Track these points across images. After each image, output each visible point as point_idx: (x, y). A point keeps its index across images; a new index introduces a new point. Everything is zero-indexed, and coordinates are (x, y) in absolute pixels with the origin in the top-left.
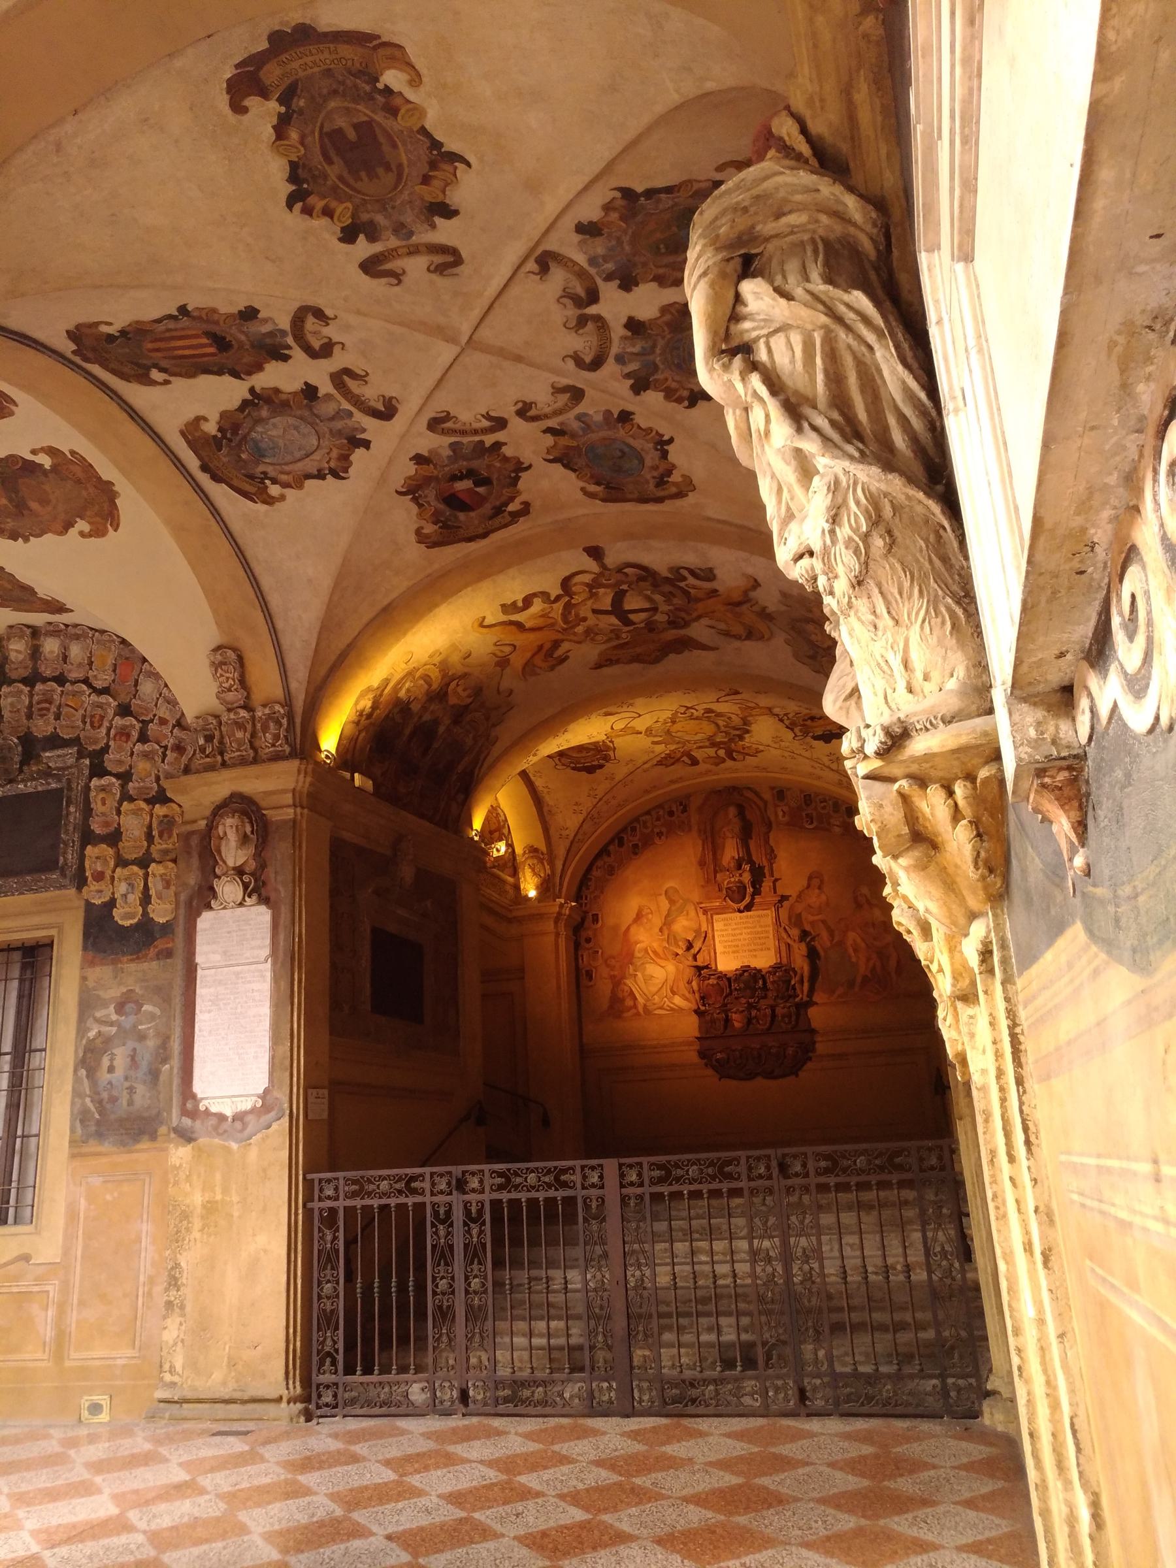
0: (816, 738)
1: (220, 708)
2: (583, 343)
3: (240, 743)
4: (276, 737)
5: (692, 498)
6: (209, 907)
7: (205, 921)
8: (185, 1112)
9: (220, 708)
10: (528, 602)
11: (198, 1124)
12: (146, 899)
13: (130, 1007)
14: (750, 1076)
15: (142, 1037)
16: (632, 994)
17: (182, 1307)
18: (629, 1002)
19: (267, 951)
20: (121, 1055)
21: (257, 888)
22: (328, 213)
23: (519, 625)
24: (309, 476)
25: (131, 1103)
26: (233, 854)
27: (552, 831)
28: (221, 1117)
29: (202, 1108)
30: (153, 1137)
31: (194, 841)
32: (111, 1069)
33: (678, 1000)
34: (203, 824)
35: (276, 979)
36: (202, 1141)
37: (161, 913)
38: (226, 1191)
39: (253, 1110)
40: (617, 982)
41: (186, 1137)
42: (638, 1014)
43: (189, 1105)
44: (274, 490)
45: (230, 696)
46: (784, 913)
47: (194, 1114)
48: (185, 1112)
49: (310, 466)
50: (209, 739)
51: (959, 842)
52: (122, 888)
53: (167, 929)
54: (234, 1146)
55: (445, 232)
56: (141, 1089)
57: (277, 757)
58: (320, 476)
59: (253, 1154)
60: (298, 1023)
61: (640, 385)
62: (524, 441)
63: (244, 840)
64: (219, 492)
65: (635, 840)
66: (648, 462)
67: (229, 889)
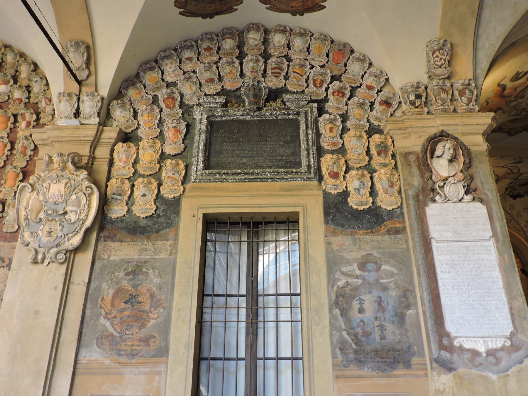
0: (511, 196)
1: (425, 80)
4: (470, 100)
7: (432, 211)
8: (442, 347)
11: (455, 357)
12: (373, 192)
13: (370, 266)
15: (385, 289)
20: (369, 301)
25: (383, 338)
28: (475, 353)
29: (456, 343)
30: (408, 365)
31: (412, 158)
32: (361, 311)
36: (461, 370)
37: (387, 202)
39: (502, 349)
41: (447, 367)
43: (445, 342)
47: (450, 349)
50: (419, 96)
52: (356, 184)
53: (391, 214)
54: (494, 377)
56: (390, 328)
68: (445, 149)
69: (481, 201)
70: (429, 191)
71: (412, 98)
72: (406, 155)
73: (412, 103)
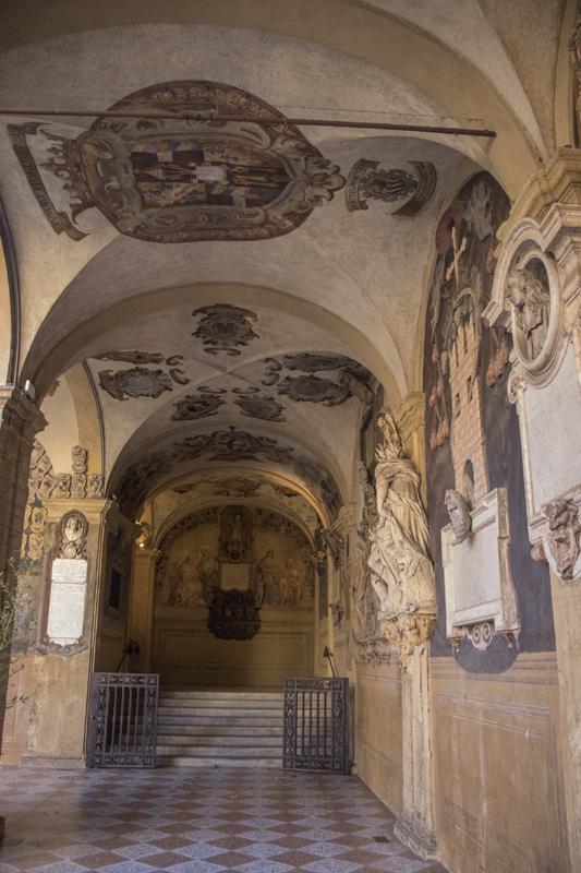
1: (72, 473)
2: (268, 379)
3: (80, 488)
5: (283, 423)
6: (59, 557)
7: (57, 563)
9: (72, 473)
10: (197, 438)
11: (48, 648)
14: (230, 638)
16: (180, 596)
17: (37, 721)
18: (178, 599)
19: (84, 580)
21: (81, 551)
22: (204, 337)
23: (189, 445)
24: (142, 395)
26: (71, 535)
27: (156, 515)
28: (59, 646)
29: (51, 641)
31: (54, 526)
33: (202, 601)
34: (58, 520)
35: (88, 591)
36: (50, 655)
38: (59, 676)
40: (173, 589)
41: (42, 652)
42: (181, 605)
44: (126, 396)
45: (78, 468)
46: (255, 567)
47: (47, 644)
48: (42, 642)
49: (144, 392)
50: (65, 484)
51: (424, 631)
54: (65, 659)
55: (239, 347)
57: (95, 497)
58: (147, 396)
59: (73, 663)
60: (96, 610)
61: (282, 392)
62: (230, 397)
63: (77, 529)
64: (102, 394)
65: (190, 523)
66: (273, 411)
67: (70, 551)
68: (72, 522)
69: (86, 558)
70: (57, 552)
71: (61, 484)
72: (51, 524)
73: (61, 488)
